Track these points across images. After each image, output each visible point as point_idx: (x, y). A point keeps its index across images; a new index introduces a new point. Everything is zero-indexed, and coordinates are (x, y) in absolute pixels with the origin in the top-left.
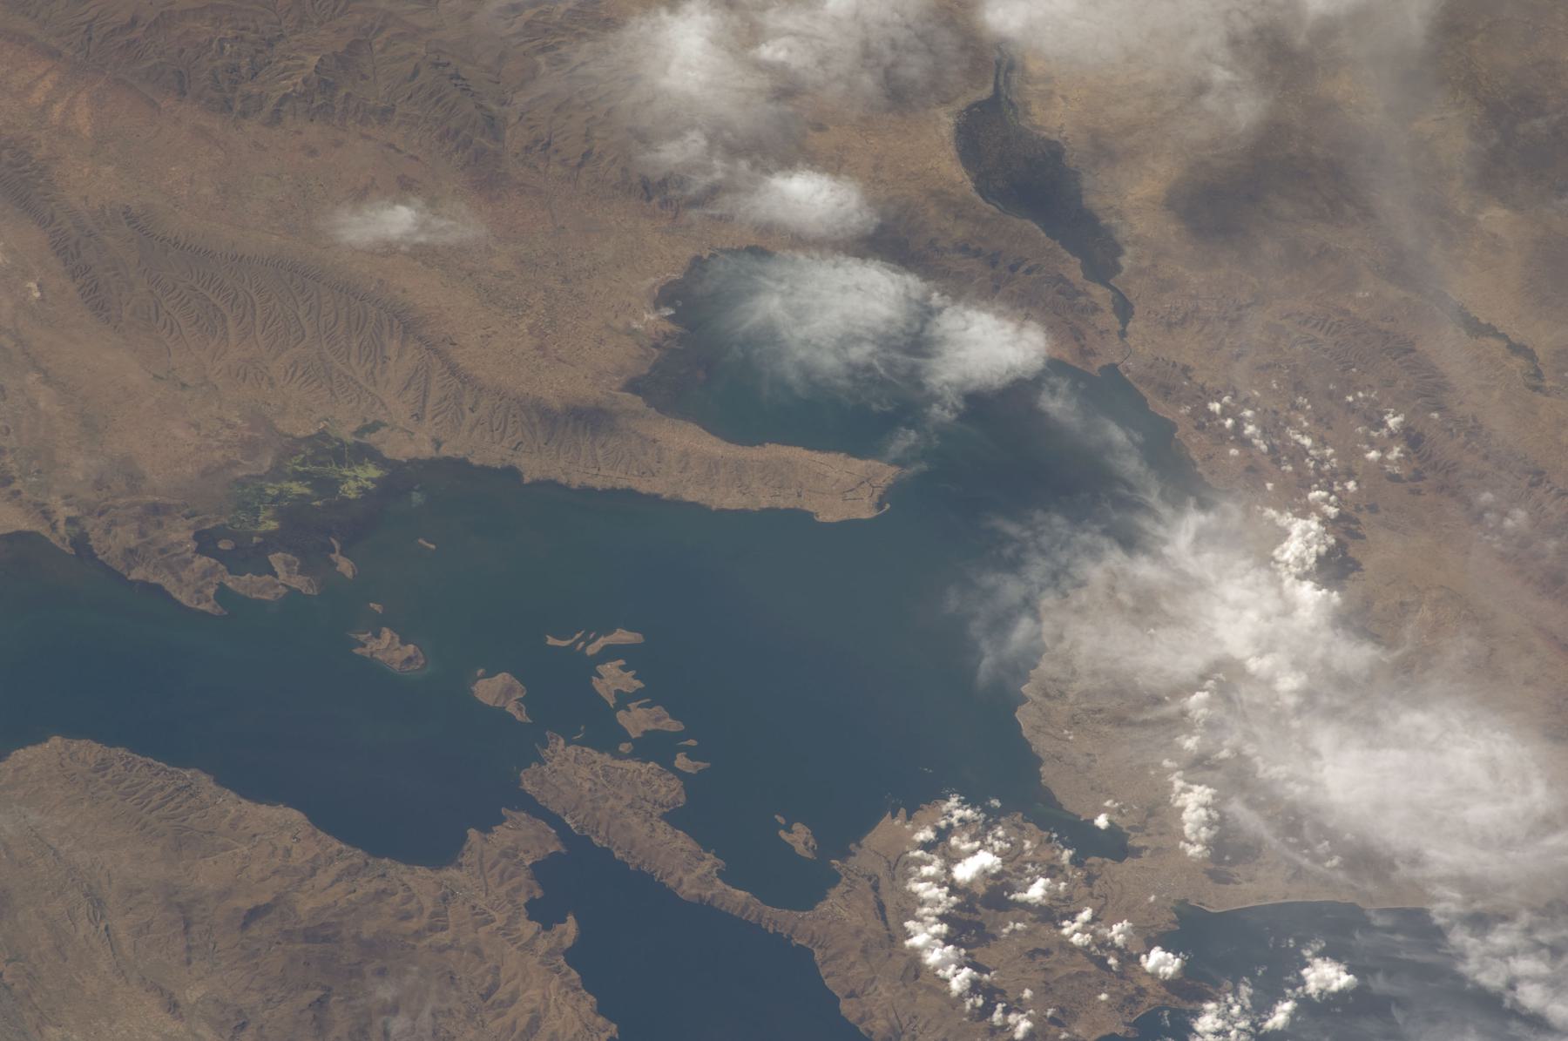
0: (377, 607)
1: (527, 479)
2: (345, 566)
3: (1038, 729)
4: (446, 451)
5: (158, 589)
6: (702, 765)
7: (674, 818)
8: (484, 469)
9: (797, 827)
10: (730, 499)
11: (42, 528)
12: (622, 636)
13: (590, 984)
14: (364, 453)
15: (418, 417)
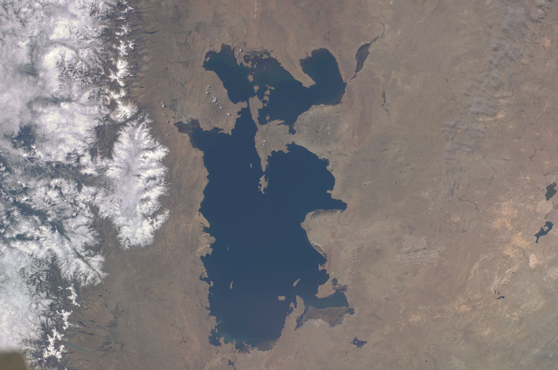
0: (254, 73)
1: (281, 66)
2: (255, 67)
3: (299, 118)
4: (276, 58)
5: (236, 59)
6: (267, 106)
7: (259, 110)
8: (278, 62)
9: (269, 117)
10: (297, 78)
11: (232, 46)
12: (273, 88)
13: (236, 123)
14: (269, 54)
15: (277, 53)
